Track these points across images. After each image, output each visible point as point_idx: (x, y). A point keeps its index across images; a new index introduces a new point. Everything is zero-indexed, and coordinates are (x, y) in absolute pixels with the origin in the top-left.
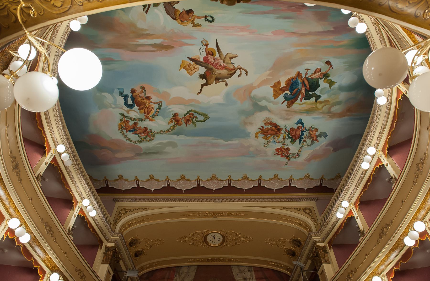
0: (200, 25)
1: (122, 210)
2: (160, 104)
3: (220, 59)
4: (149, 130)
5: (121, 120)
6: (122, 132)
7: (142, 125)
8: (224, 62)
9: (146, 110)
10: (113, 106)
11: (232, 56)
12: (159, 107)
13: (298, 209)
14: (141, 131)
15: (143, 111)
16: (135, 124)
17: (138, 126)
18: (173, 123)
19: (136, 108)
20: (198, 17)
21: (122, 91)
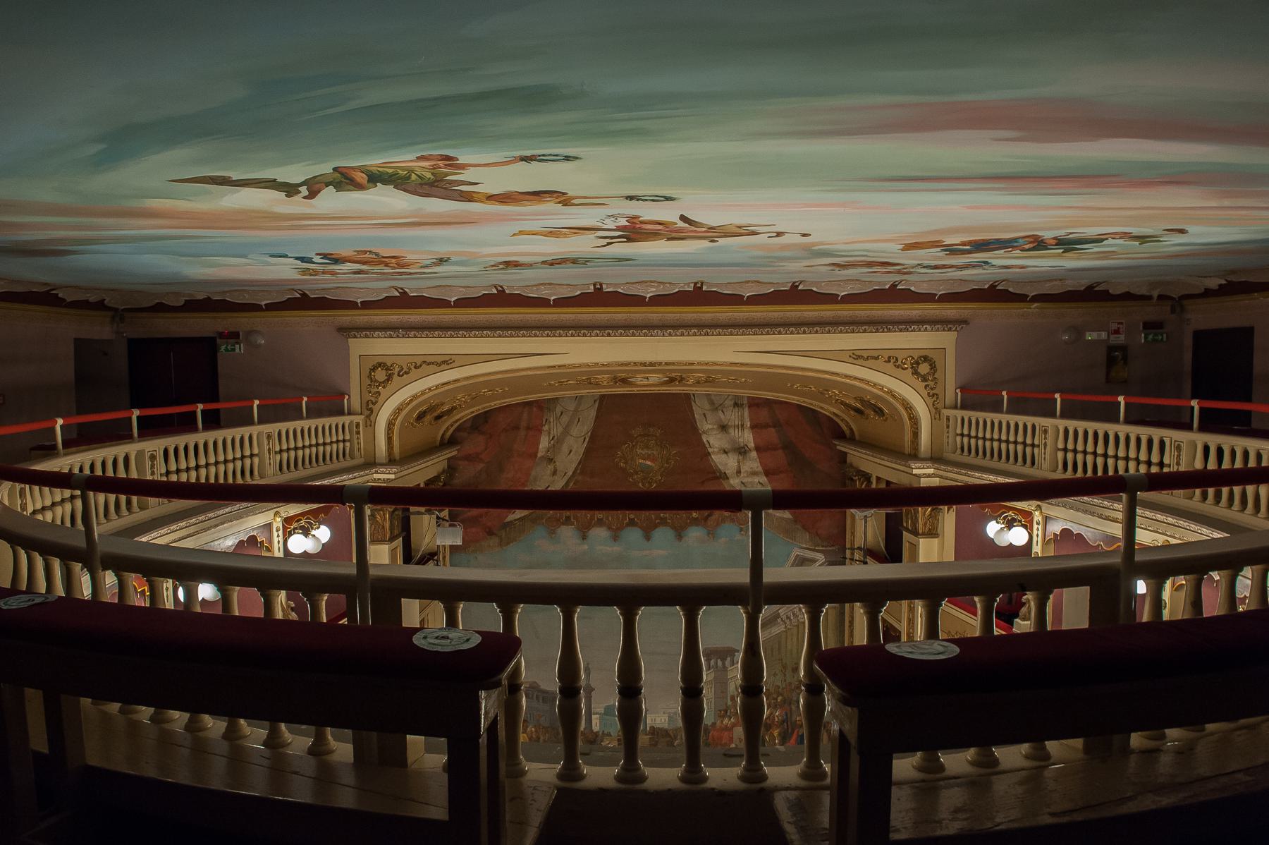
1: (374, 369)
13: (893, 360)
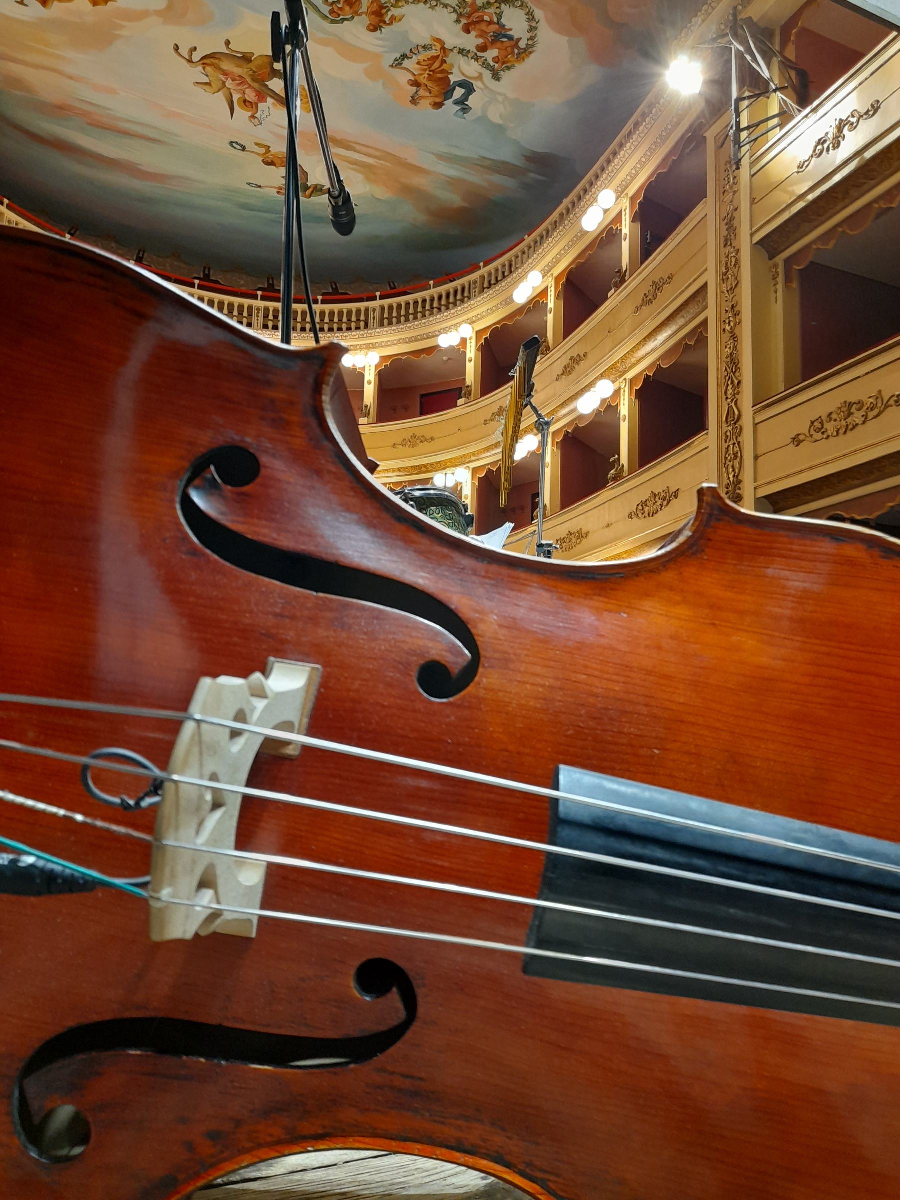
0: (257, 144)
2: (398, 63)
3: (232, 91)
4: (464, 21)
5: (509, 69)
6: (530, 43)
7: (471, 41)
8: (224, 83)
9: (437, 65)
10: (500, 99)
11: (207, 88)
12: (403, 60)
14: (483, 27)
15: (445, 67)
16: (483, 48)
17: (481, 41)
18: (390, 14)
19: (453, 79)
20: (258, 154)
21: (461, 114)
